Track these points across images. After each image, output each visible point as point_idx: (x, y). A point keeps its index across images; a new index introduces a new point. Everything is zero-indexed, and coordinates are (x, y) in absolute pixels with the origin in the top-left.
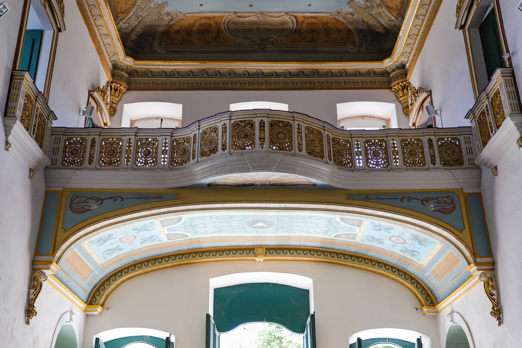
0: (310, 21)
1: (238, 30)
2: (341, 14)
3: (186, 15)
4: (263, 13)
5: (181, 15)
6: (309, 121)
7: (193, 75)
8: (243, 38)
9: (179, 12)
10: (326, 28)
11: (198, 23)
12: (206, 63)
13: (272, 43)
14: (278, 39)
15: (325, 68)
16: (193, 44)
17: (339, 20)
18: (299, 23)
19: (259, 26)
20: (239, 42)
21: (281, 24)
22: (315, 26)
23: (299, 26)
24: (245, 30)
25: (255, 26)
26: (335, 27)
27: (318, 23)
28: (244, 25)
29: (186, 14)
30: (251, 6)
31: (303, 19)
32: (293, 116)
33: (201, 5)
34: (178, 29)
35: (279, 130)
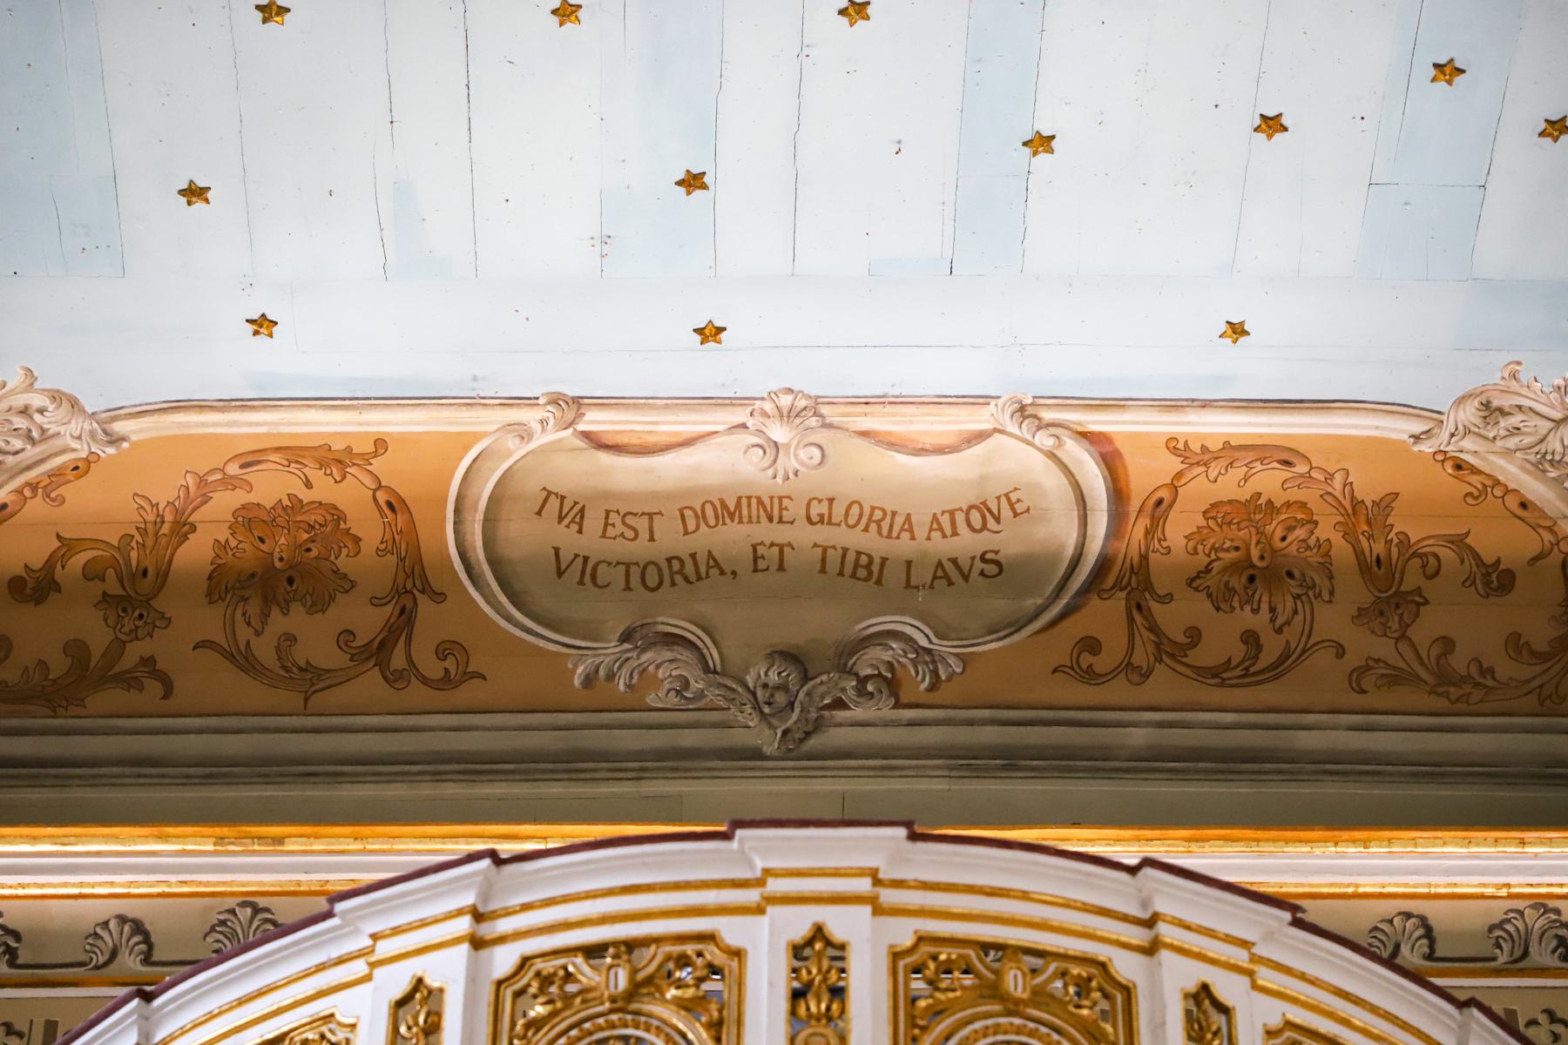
0: (1229, 485)
1: (589, 572)
2: (1515, 420)
3: (119, 427)
4: (816, 405)
5: (76, 426)
6: (1303, 977)
7: (147, 960)
8: (626, 637)
9: (57, 396)
10: (1379, 548)
11: (225, 503)
12: (279, 840)
13: (891, 684)
14: (941, 646)
15: (1368, 885)
16: (166, 696)
17: (1497, 483)
18: (1135, 505)
19: (781, 534)
20: (589, 681)
21: (976, 518)
22: (1275, 529)
23: (1137, 532)
24: (651, 570)
25: (732, 539)
26: (1459, 542)
27: (1304, 505)
28: (642, 524)
29: (116, 414)
30: (710, 333)
31: (1176, 464)
32: (1145, 904)
33: (262, 324)
34: (37, 562)
35: (997, 1029)
